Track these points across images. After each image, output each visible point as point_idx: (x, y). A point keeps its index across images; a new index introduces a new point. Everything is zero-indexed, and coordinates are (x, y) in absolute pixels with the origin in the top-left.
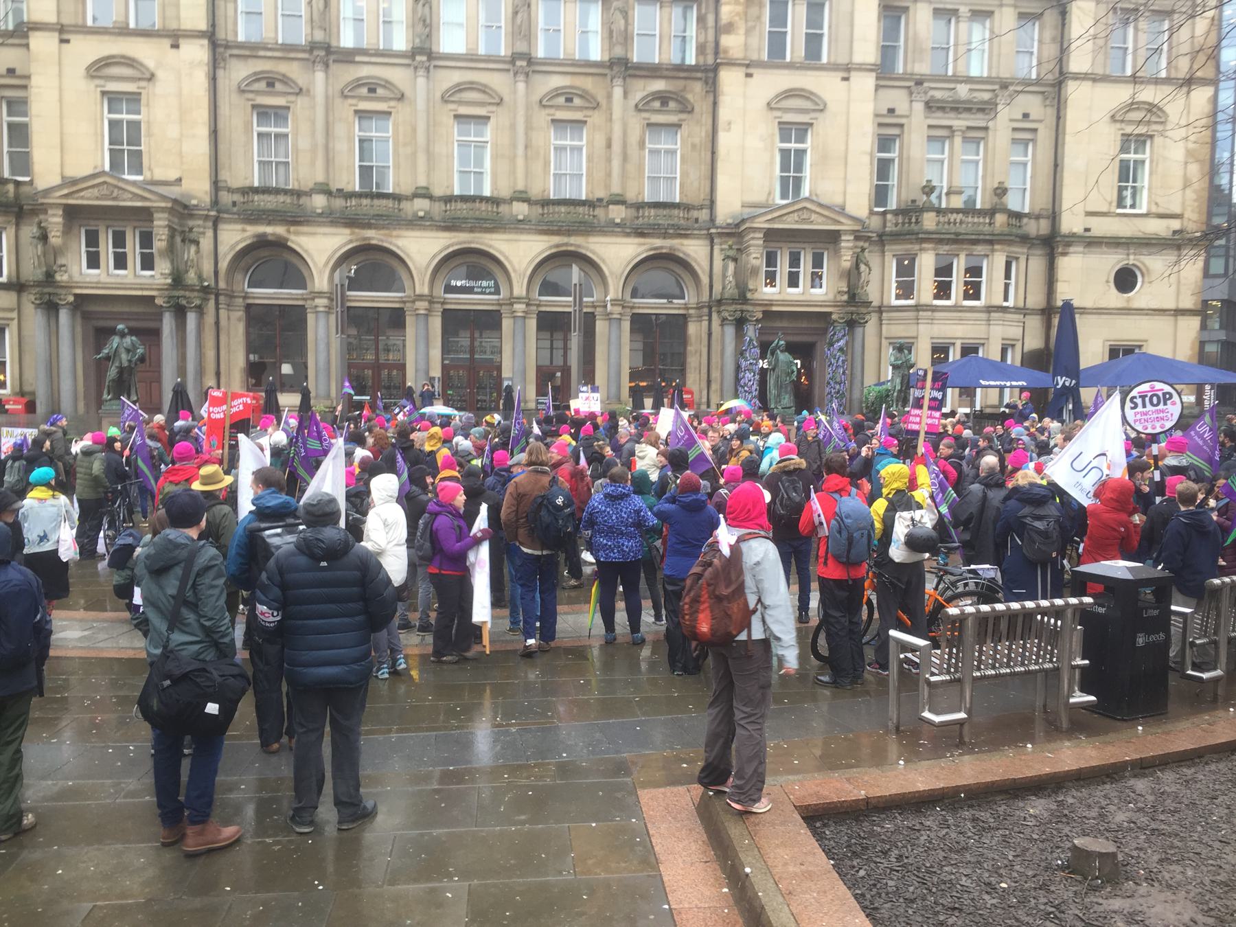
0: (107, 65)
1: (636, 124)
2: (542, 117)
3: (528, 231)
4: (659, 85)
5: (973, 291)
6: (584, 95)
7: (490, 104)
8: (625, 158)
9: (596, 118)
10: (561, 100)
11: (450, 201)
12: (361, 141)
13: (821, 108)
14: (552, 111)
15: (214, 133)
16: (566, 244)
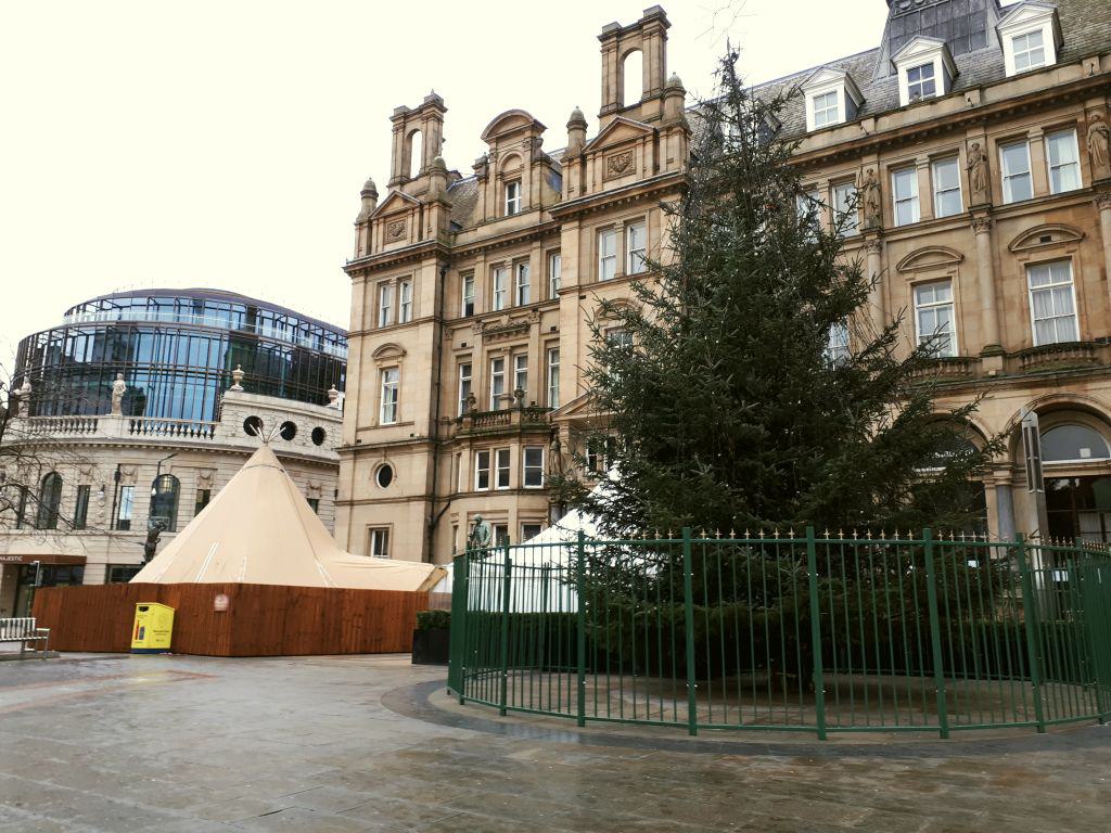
0: (383, 351)
2: (1013, 265)
3: (1004, 388)
5: (504, 480)
6: (1064, 231)
7: (950, 264)
9: (1085, 251)
10: (1036, 242)
11: (1028, 356)
12: (464, 383)
14: (1025, 256)
16: (1056, 396)
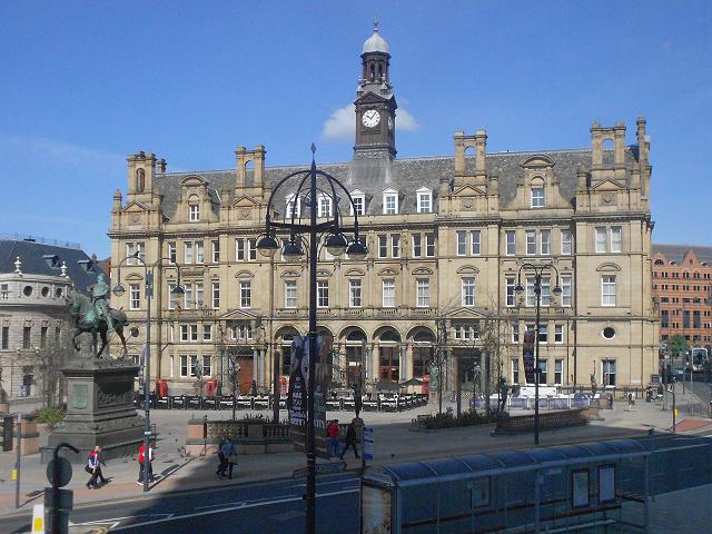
1: (412, 279)
4: (421, 265)
8: (408, 291)
13: (477, 271)
15: (272, 292)
